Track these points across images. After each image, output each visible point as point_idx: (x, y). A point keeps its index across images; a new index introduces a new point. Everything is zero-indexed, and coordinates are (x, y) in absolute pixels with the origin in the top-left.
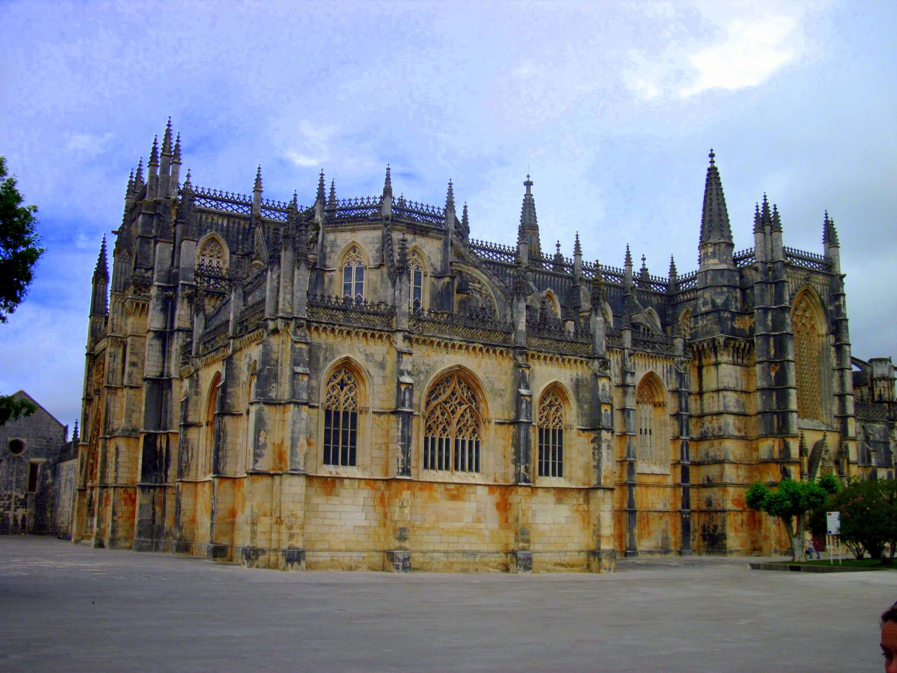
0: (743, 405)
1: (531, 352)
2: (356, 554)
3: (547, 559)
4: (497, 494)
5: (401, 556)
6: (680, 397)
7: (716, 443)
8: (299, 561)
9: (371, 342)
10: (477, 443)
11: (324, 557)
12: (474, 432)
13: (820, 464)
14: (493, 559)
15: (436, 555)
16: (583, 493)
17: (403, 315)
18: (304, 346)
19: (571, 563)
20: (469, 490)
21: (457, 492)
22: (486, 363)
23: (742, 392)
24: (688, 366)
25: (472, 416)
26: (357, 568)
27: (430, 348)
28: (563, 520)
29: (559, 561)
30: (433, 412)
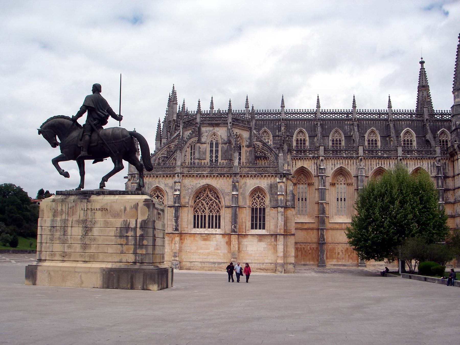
4: (226, 238)
5: (174, 263)
6: (438, 180)
9: (167, 179)
10: (219, 216)
12: (218, 211)
15: (196, 263)
16: (274, 237)
17: (178, 166)
18: (135, 184)
20: (212, 236)
21: (207, 237)
24: (447, 161)
25: (217, 205)
27: (193, 178)
28: (262, 249)
30: (198, 205)
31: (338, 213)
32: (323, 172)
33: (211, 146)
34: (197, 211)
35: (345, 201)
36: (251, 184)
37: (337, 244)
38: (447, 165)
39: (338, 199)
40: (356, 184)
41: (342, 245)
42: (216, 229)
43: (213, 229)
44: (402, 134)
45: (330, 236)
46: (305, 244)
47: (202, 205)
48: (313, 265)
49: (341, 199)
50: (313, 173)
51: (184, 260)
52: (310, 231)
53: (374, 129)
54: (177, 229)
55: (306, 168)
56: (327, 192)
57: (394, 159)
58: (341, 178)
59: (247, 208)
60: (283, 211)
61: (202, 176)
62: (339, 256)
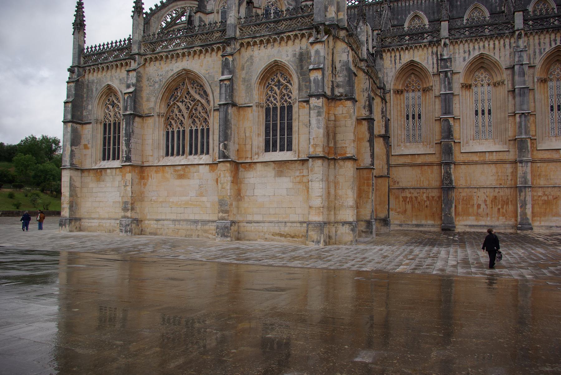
1: (246, 40)
2: (113, 221)
3: (265, 229)
5: (123, 223)
10: (208, 130)
11: (95, 223)
15: (166, 222)
19: (293, 235)
20: (192, 169)
21: (183, 172)
22: (208, 61)
26: (114, 231)
29: (278, 232)
31: (478, 135)
32: (448, 64)
34: (171, 125)
35: (489, 114)
36: (261, 56)
37: (476, 190)
39: (477, 112)
40: (510, 82)
41: (485, 190)
43: (196, 157)
45: (460, 176)
46: (418, 191)
47: (180, 111)
48: (433, 226)
49: (483, 111)
50: (430, 70)
51: (148, 217)
52: (426, 167)
55: (417, 63)
56: (456, 100)
58: (482, 75)
60: (320, 105)
61: (174, 56)
62: (481, 210)
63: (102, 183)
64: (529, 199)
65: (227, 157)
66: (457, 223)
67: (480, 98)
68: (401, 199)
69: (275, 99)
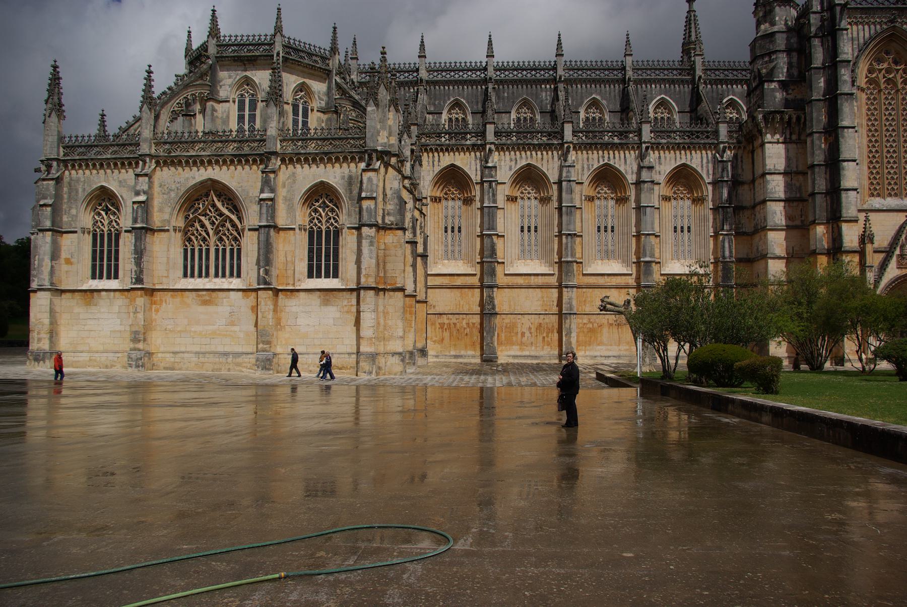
0: (799, 189)
2: (112, 355)
3: (310, 361)
5: (133, 356)
7: (762, 233)
8: (44, 360)
10: (239, 251)
13: (897, 252)
14: (246, 360)
15: (186, 355)
16: (355, 294)
18: (51, 182)
19: (340, 366)
20: (220, 293)
23: (798, 173)
26: (112, 366)
32: (493, 173)
33: (241, 108)
34: (190, 240)
38: (739, 160)
39: (522, 228)
42: (231, 280)
43: (224, 280)
44: (651, 108)
45: (502, 300)
47: (203, 226)
50: (473, 177)
51: (162, 349)
53: (598, 97)
54: (139, 280)
56: (500, 213)
57: (633, 148)
59: (297, 230)
60: (373, 234)
62: (525, 339)
63: (94, 307)
64: (573, 326)
65: (269, 284)
66: (499, 353)
67: (526, 214)
68: (438, 326)
69: (320, 222)
